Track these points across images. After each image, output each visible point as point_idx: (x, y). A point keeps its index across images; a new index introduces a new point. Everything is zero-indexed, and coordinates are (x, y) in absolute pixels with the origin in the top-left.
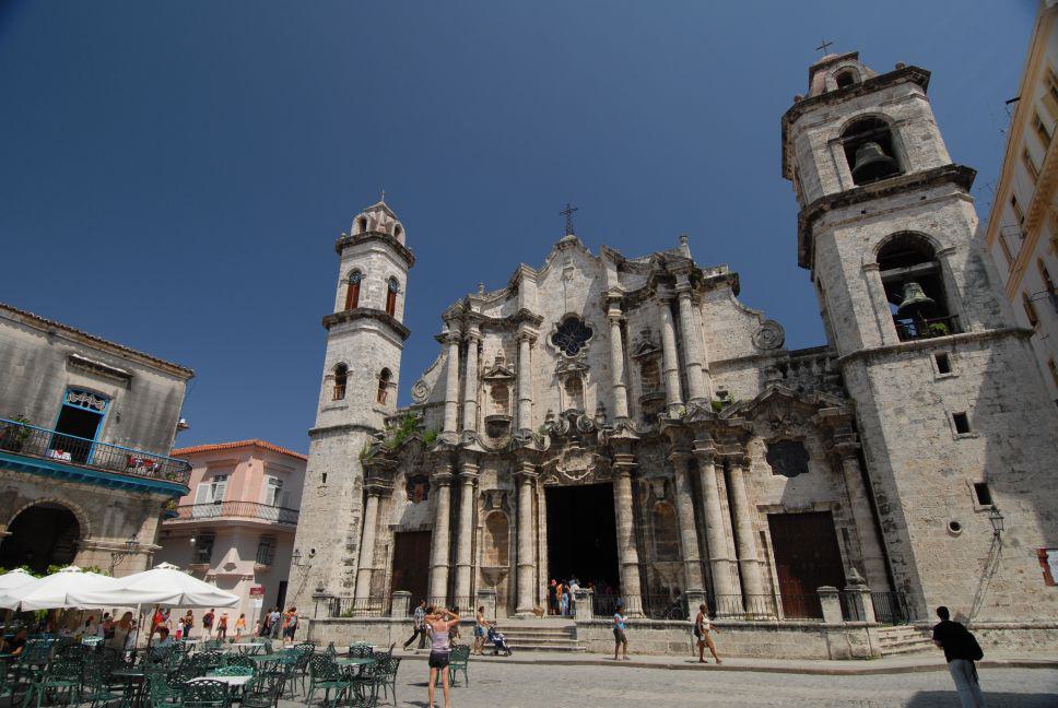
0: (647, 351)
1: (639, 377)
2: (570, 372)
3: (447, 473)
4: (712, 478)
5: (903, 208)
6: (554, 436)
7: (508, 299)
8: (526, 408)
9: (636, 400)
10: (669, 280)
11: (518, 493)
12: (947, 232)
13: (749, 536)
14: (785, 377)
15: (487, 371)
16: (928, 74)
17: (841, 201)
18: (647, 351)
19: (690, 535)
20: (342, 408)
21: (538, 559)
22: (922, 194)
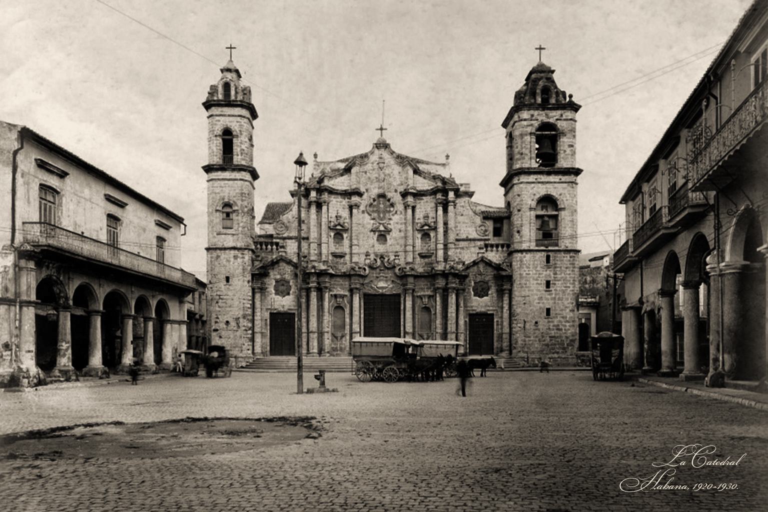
0: (426, 227)
1: (420, 240)
2: (381, 231)
3: (315, 284)
4: (452, 299)
5: (551, 183)
6: (371, 267)
7: (342, 175)
8: (355, 250)
9: (417, 253)
10: (445, 192)
11: (352, 296)
12: (564, 199)
13: (462, 322)
14: (487, 251)
15: (332, 224)
16: (580, 107)
17: (528, 172)
18: (426, 227)
19: (439, 321)
20: (233, 235)
21: (360, 329)
22: (560, 177)
